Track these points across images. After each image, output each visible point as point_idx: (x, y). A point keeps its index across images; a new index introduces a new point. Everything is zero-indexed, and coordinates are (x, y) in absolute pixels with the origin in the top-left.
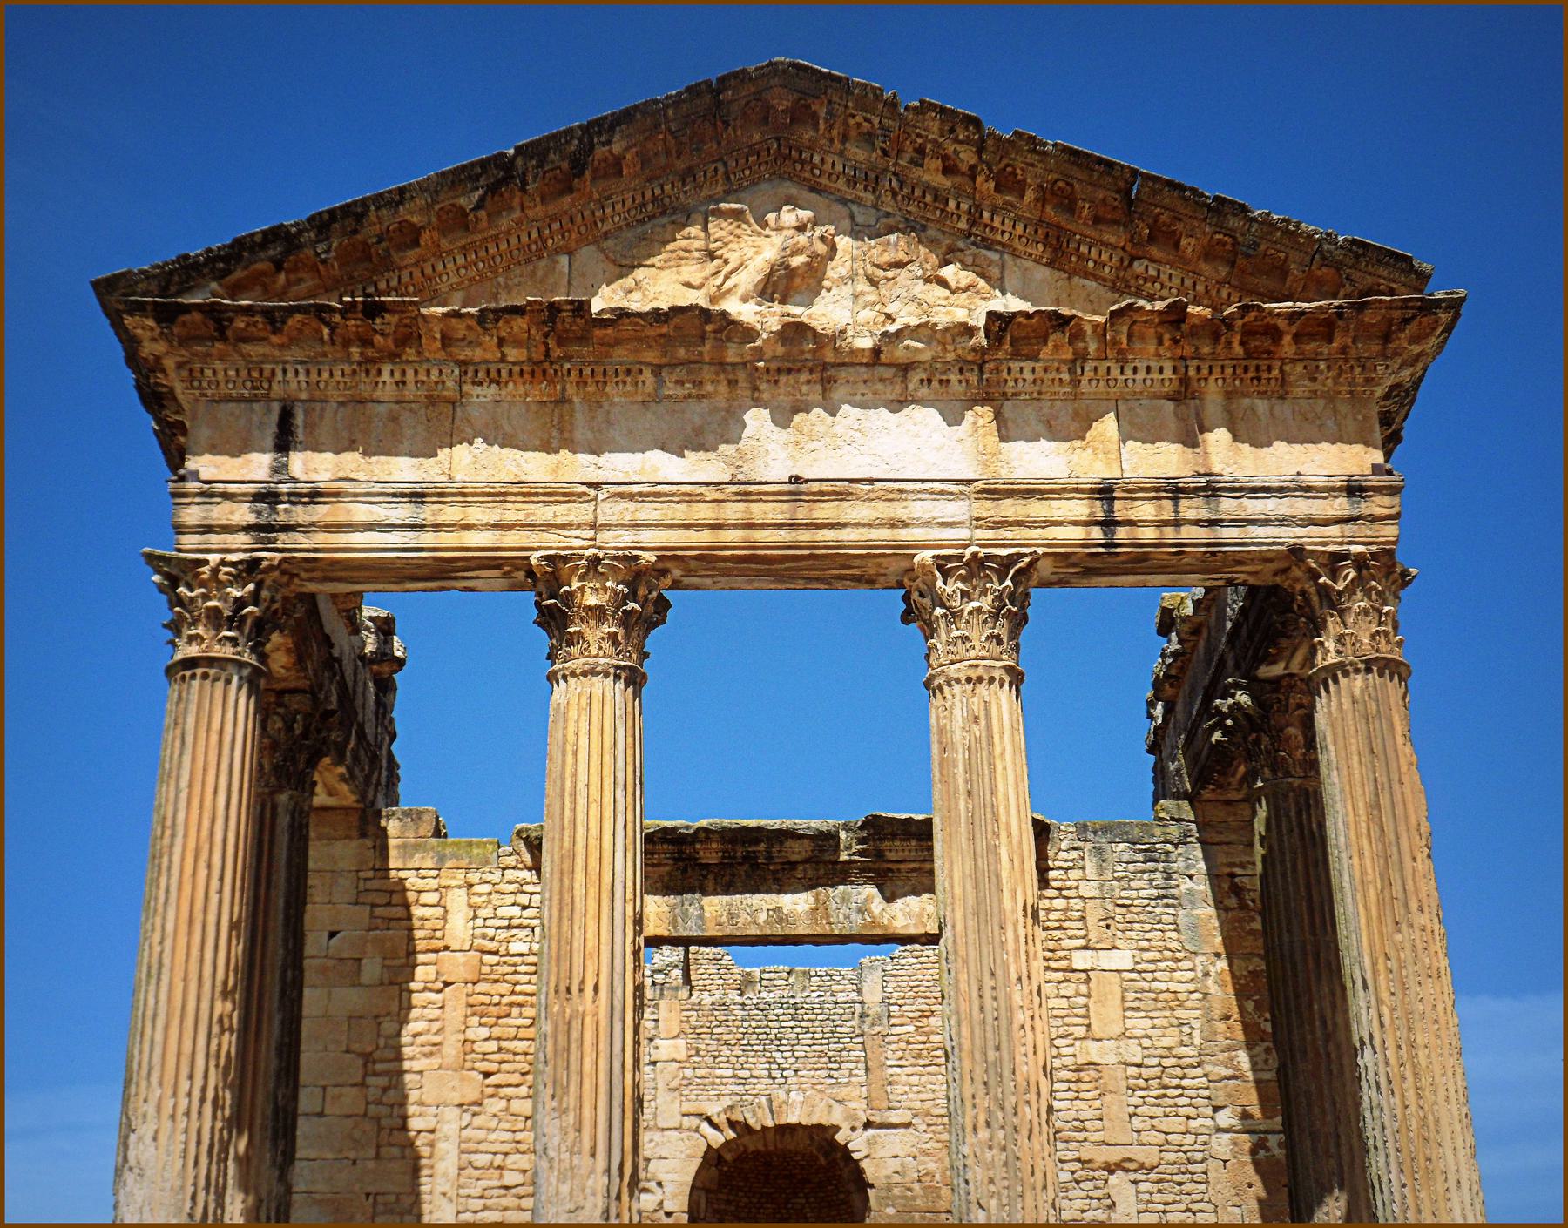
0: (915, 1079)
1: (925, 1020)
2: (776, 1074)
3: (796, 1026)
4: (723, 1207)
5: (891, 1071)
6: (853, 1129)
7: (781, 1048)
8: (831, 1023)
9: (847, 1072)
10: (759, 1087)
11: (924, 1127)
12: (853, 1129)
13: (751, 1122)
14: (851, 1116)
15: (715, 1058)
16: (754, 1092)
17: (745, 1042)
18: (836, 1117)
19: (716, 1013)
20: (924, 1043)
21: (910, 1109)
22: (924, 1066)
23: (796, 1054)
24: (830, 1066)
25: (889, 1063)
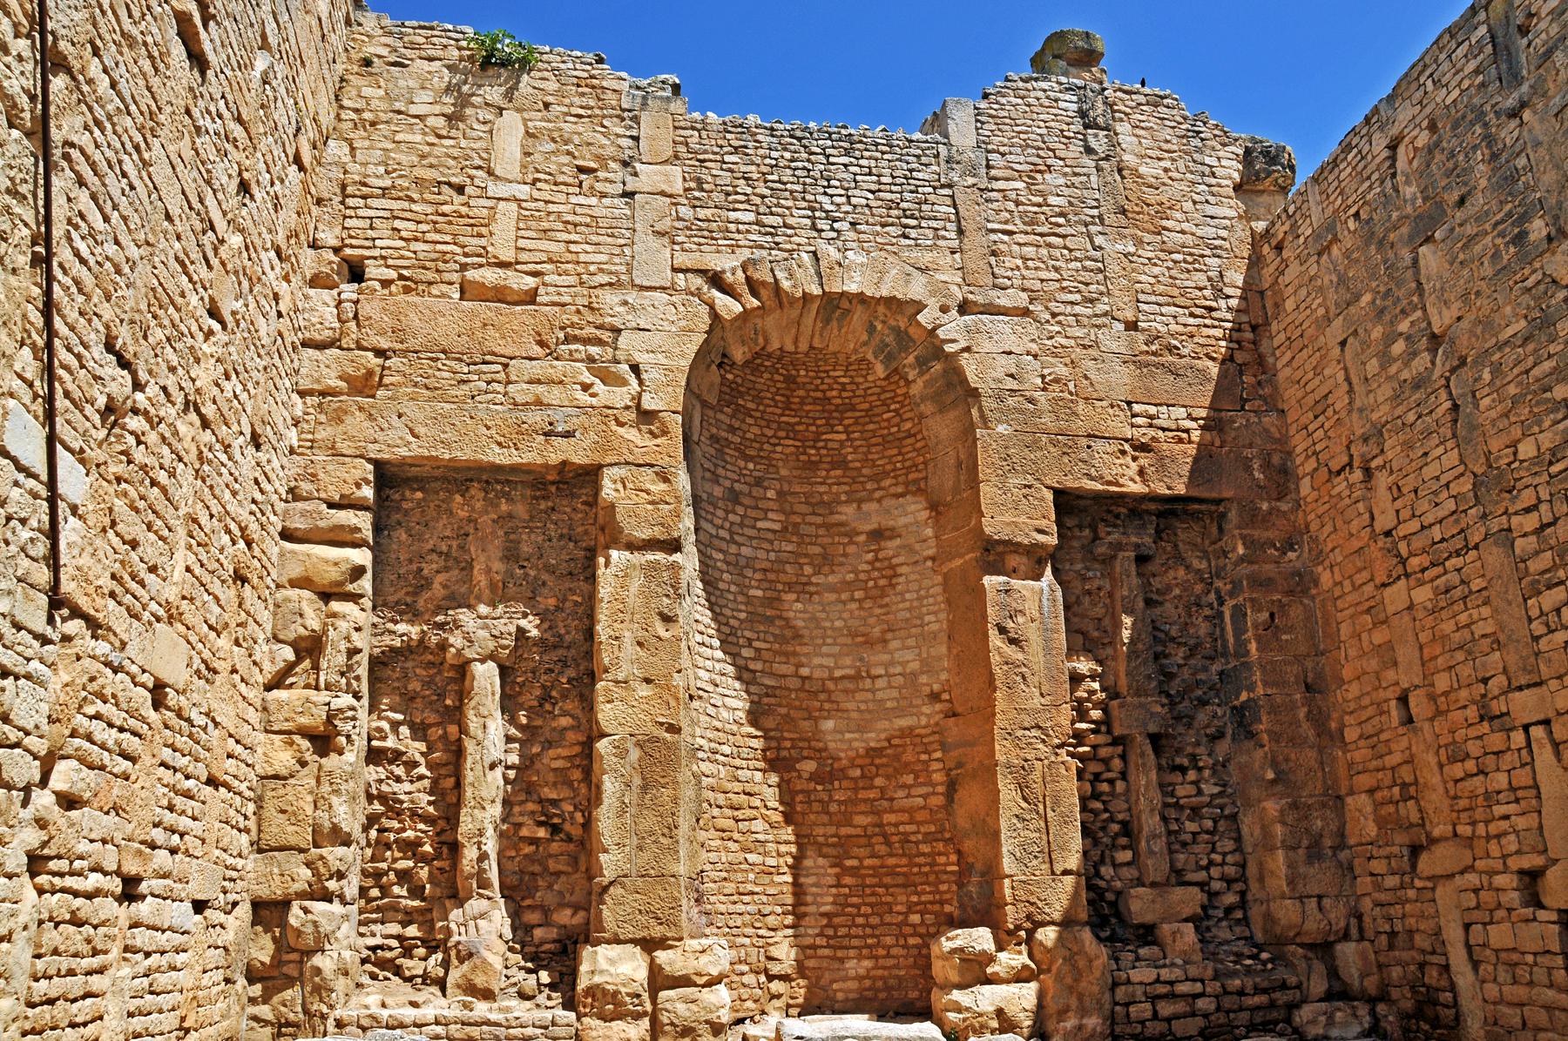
0: (1029, 251)
1: (1038, 176)
2: (822, 224)
3: (852, 164)
4: (724, 434)
5: (993, 237)
6: (944, 309)
7: (829, 191)
8: (905, 166)
9: (930, 233)
10: (795, 239)
11: (1048, 317)
12: (944, 309)
13: (786, 284)
14: (939, 289)
15: (728, 194)
16: (788, 246)
17: (775, 177)
18: (916, 289)
19: (729, 136)
20: (1040, 205)
21: (1024, 290)
22: (1042, 235)
23: (854, 200)
24: (904, 221)
25: (990, 226)
